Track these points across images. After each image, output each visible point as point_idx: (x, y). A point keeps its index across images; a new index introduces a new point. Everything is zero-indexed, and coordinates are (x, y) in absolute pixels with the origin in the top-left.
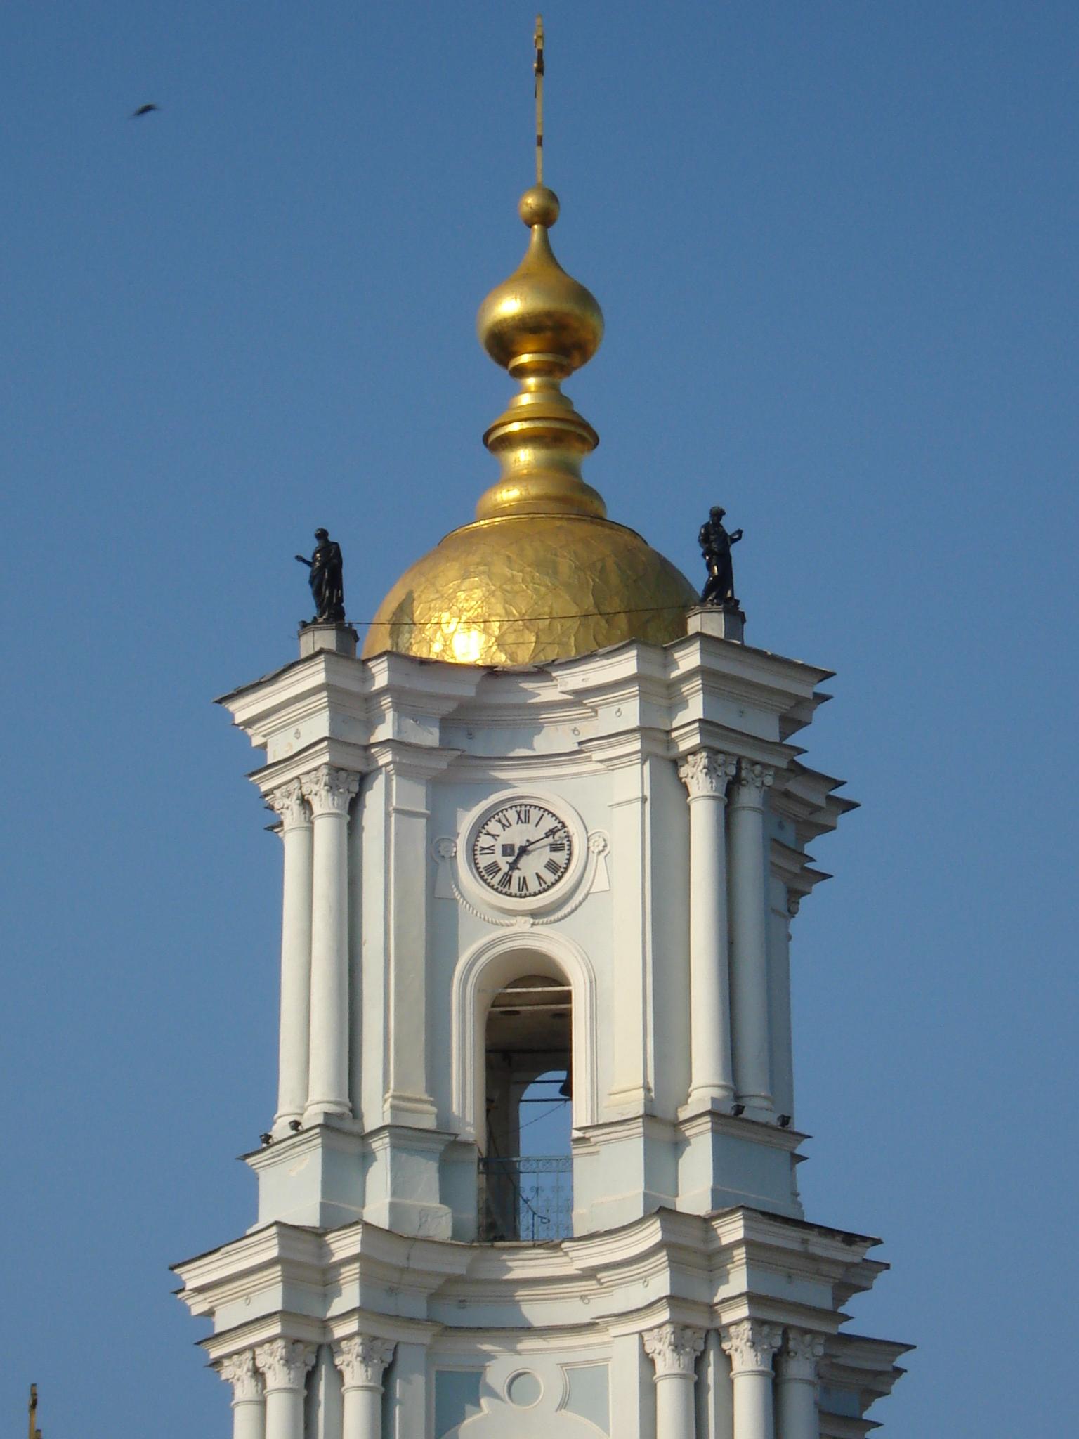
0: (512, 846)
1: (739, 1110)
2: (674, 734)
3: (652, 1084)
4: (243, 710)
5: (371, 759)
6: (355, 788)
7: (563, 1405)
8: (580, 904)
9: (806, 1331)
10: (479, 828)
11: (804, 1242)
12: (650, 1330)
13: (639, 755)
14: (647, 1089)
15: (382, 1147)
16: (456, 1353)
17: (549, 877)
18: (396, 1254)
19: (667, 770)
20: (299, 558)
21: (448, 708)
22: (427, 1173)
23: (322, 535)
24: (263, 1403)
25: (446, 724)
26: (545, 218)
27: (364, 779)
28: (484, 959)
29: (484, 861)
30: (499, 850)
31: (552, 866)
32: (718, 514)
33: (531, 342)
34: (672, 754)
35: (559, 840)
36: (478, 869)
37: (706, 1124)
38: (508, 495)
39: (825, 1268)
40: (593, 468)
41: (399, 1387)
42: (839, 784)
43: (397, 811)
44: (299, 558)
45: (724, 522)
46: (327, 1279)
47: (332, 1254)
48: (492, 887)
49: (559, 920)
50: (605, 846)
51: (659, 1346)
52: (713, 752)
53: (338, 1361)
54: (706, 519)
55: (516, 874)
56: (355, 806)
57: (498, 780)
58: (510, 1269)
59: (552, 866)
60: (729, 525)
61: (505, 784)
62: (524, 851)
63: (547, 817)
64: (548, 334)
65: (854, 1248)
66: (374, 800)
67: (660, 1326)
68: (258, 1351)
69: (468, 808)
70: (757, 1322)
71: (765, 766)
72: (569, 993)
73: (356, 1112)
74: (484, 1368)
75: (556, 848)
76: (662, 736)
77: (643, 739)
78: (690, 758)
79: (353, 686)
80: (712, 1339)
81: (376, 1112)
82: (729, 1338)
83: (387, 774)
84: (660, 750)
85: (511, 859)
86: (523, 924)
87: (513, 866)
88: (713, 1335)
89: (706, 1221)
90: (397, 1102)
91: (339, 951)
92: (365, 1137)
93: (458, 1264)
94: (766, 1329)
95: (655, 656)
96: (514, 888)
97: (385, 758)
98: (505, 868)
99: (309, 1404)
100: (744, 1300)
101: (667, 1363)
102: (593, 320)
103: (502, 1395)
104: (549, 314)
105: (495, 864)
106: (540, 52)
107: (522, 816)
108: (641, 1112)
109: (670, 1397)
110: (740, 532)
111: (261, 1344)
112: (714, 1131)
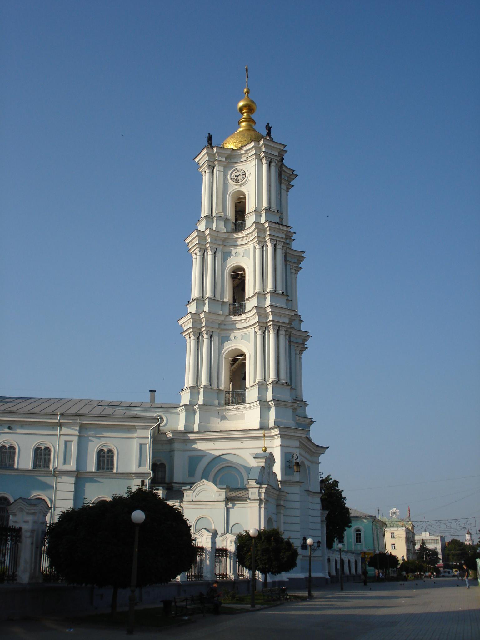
1: (270, 209)
4: (197, 160)
6: (213, 168)
7: (243, 256)
9: (280, 241)
10: (232, 173)
11: (279, 227)
12: (255, 242)
14: (256, 207)
15: (215, 219)
16: (227, 250)
17: (242, 179)
18: (216, 234)
21: (226, 155)
22: (222, 224)
23: (209, 134)
25: (226, 158)
27: (214, 167)
28: (232, 193)
29: (232, 178)
30: (235, 176)
31: (243, 178)
32: (268, 124)
33: (245, 108)
34: (260, 158)
35: (244, 174)
37: (264, 211)
38: (241, 129)
45: (269, 125)
47: (206, 234)
51: (256, 244)
52: (266, 157)
54: (267, 124)
55: (237, 179)
56: (213, 171)
57: (234, 166)
59: (243, 178)
60: (270, 125)
61: (236, 166)
62: (238, 176)
63: (242, 170)
65: (288, 228)
66: (215, 170)
67: (256, 241)
72: (245, 197)
74: (231, 252)
79: (211, 153)
81: (214, 214)
82: (267, 242)
84: (258, 158)
86: (238, 187)
87: (237, 178)
90: (218, 213)
93: (226, 236)
94: (273, 240)
95: (257, 143)
96: (237, 181)
97: (216, 163)
98: (235, 178)
101: (257, 246)
102: (254, 105)
103: (233, 255)
104: (247, 104)
108: (254, 209)
109: (258, 252)
110: (272, 126)
111: (195, 249)
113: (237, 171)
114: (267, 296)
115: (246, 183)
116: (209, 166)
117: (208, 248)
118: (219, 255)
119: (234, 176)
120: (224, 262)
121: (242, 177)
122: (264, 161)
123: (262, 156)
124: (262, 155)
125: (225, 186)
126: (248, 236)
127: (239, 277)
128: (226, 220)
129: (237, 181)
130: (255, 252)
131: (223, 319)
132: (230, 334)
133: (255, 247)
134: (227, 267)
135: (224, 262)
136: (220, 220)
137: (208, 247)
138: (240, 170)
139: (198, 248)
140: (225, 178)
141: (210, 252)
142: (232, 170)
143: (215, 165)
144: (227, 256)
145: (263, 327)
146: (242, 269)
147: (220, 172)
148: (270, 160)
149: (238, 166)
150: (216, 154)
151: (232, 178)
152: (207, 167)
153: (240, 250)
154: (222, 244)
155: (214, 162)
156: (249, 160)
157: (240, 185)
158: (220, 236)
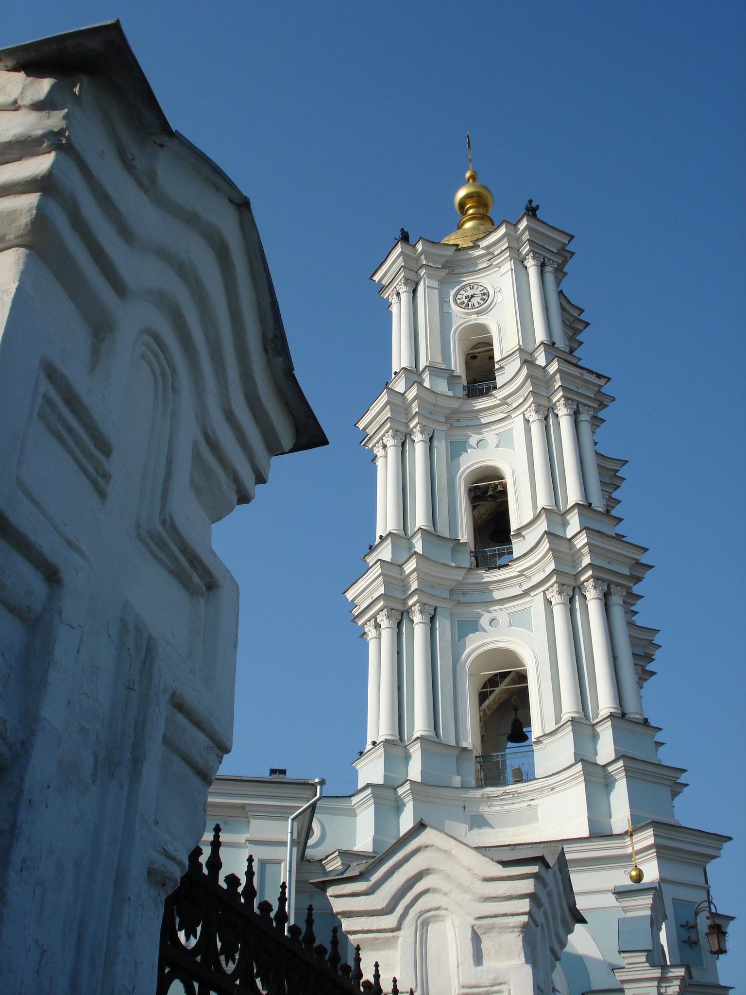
0: (469, 296)
2: (520, 250)
4: (377, 278)
6: (414, 286)
7: (497, 446)
8: (493, 307)
9: (585, 405)
11: (582, 374)
12: (526, 410)
13: (509, 258)
16: (457, 435)
17: (482, 302)
18: (431, 399)
19: (519, 264)
21: (444, 260)
24: (386, 457)
27: (417, 284)
29: (459, 302)
30: (464, 298)
31: (482, 299)
32: (531, 201)
35: (485, 295)
36: (457, 304)
37: (542, 348)
39: (590, 386)
41: (435, 443)
42: (582, 311)
48: (463, 308)
49: (486, 314)
50: (500, 290)
52: (535, 253)
55: (470, 303)
56: (415, 291)
62: (472, 296)
64: (475, 198)
65: (601, 380)
68: (384, 438)
69: (453, 290)
70: (567, 399)
71: (554, 261)
74: (468, 439)
76: (517, 252)
78: (527, 257)
79: (411, 254)
80: (550, 410)
81: (423, 363)
83: (424, 278)
84: (517, 257)
86: (474, 316)
88: (550, 410)
89: (544, 368)
91: (410, 327)
92: (420, 375)
93: (456, 404)
98: (466, 301)
99: (403, 453)
100: (560, 389)
101: (533, 416)
102: (489, 196)
103: (474, 445)
105: (463, 301)
106: (468, 135)
107: (472, 288)
108: (518, 347)
110: (538, 206)
111: (384, 435)
113: (468, 288)
114: (568, 518)
116: (407, 281)
117: (414, 430)
118: (440, 446)
119: (461, 298)
120: (452, 460)
121: (481, 298)
122: (530, 263)
123: (524, 253)
124: (525, 249)
125: (445, 318)
126: (507, 404)
127: (490, 493)
128: (452, 378)
129: (470, 307)
130: (528, 431)
131: (461, 579)
132: (480, 616)
134: (460, 471)
135: (452, 460)
136: (438, 377)
137: (415, 427)
138: (476, 287)
139: (391, 431)
140: (443, 301)
141: (418, 437)
142: (458, 287)
143: (422, 278)
144: (457, 449)
145: (569, 586)
146: (494, 475)
147: (431, 290)
149: (469, 279)
150: (423, 257)
151: (459, 302)
152: (403, 281)
153: (490, 436)
154: (446, 422)
155: (417, 272)
156: (494, 263)
157: (478, 313)
158: (440, 404)
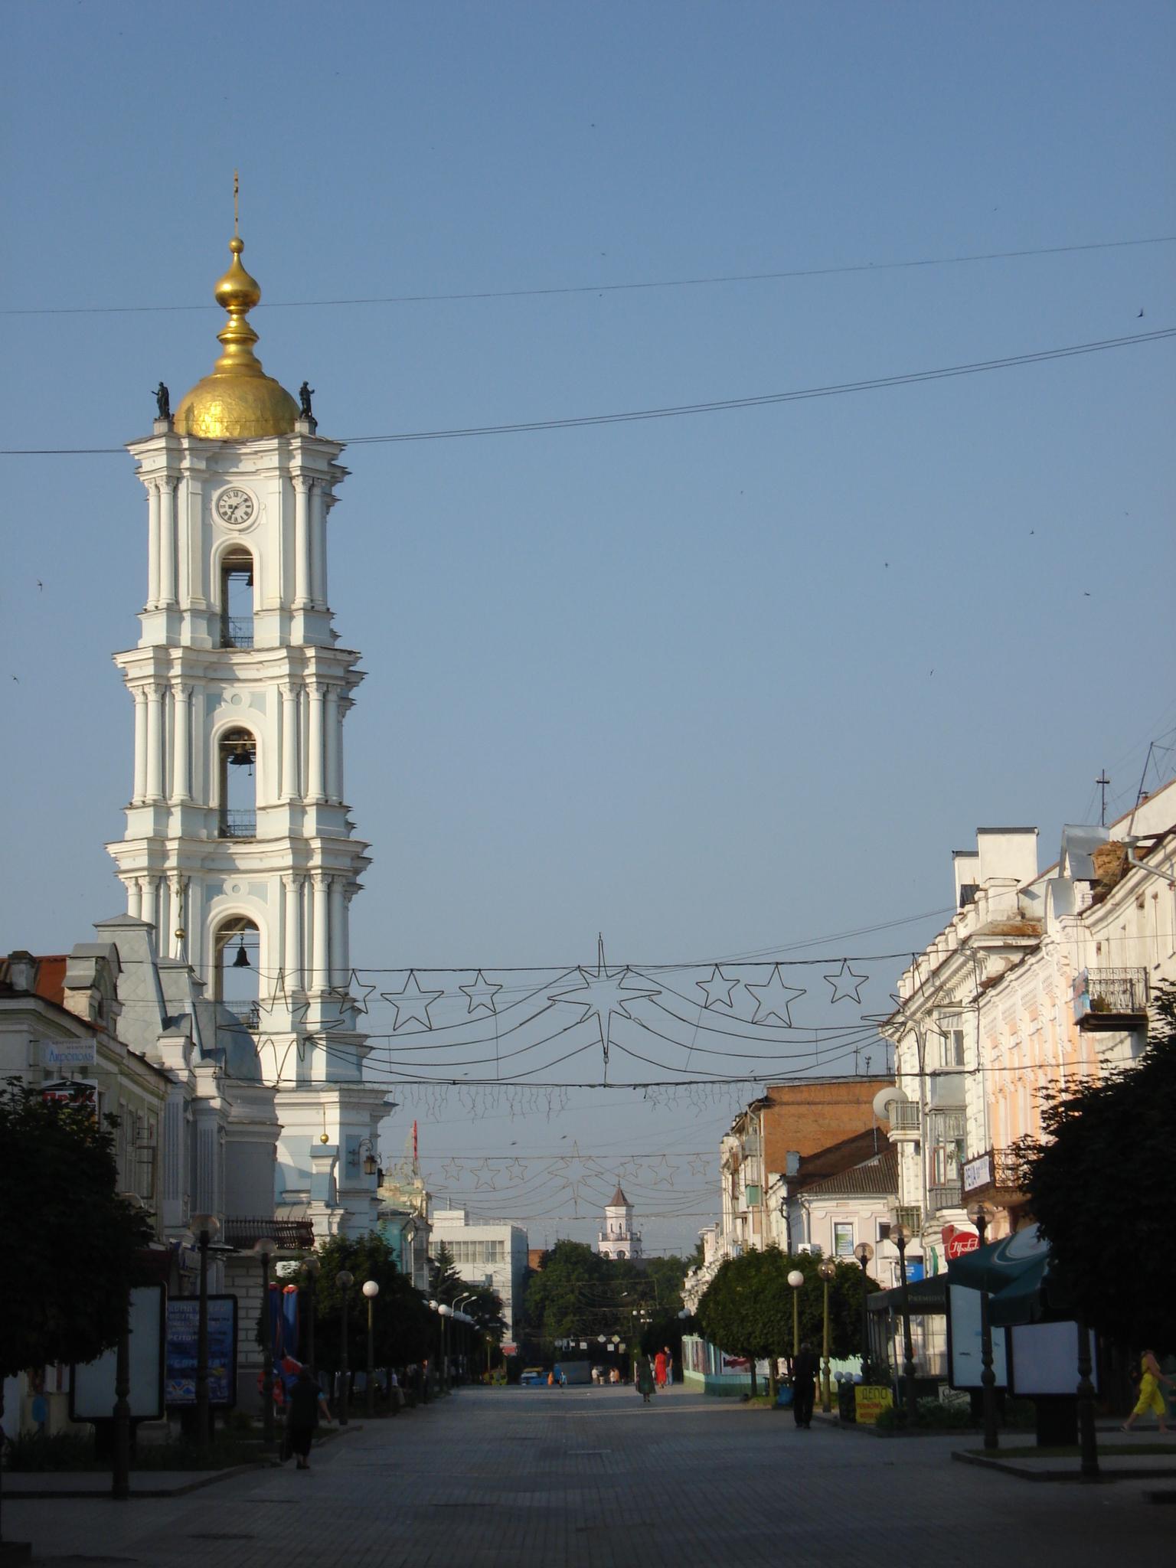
3: (282, 596)
5: (181, 473)
7: (250, 706)
9: (334, 684)
10: (220, 498)
11: (335, 655)
14: (281, 598)
15: (187, 616)
17: (245, 517)
20: (153, 392)
21: (209, 454)
22: (203, 624)
23: (161, 384)
25: (208, 460)
26: (246, 300)
27: (179, 479)
28: (222, 547)
29: (222, 510)
30: (227, 507)
31: (246, 513)
32: (306, 384)
38: (227, 362)
40: (258, 350)
41: (194, 700)
43: (191, 493)
44: (153, 392)
45: (308, 386)
46: (169, 663)
51: (285, 690)
53: (173, 691)
54: (302, 385)
55: (233, 516)
56: (175, 490)
57: (228, 481)
58: (232, 659)
59: (246, 513)
60: (310, 388)
61: (229, 482)
62: (236, 507)
66: (183, 488)
69: (215, 490)
73: (177, 602)
75: (248, 507)
77: (280, 471)
81: (185, 603)
84: (285, 474)
85: (232, 510)
87: (233, 513)
91: (171, 543)
93: (214, 658)
96: (233, 521)
97: (187, 474)
98: (229, 513)
104: (241, 291)
112: (304, 615)
113: (232, 494)
115: (255, 529)
118: (199, 701)
121: (244, 511)
130: (281, 704)
132: (224, 880)
133: (280, 694)
134: (214, 729)
135: (207, 715)
138: (240, 494)
144: (213, 702)
148: (311, 482)
149: (237, 482)
